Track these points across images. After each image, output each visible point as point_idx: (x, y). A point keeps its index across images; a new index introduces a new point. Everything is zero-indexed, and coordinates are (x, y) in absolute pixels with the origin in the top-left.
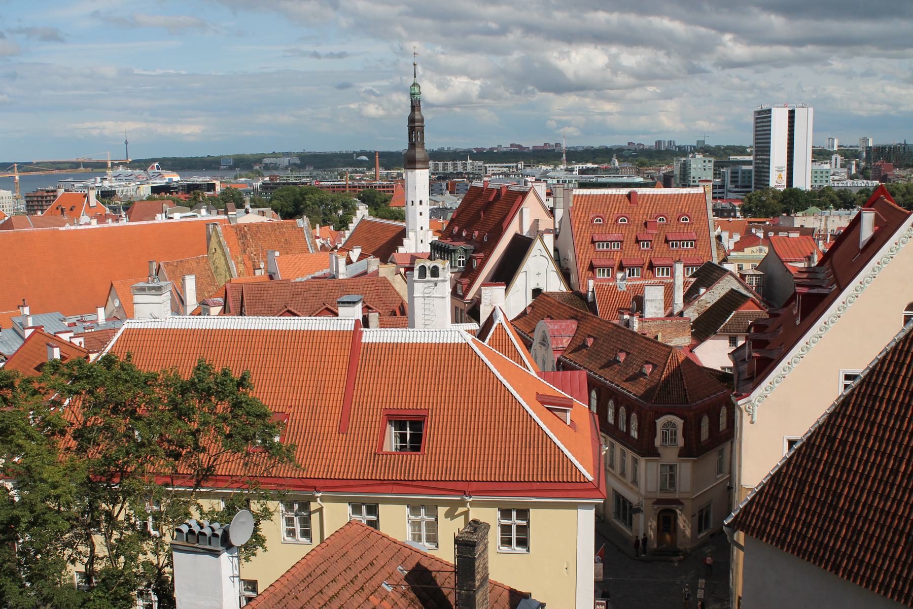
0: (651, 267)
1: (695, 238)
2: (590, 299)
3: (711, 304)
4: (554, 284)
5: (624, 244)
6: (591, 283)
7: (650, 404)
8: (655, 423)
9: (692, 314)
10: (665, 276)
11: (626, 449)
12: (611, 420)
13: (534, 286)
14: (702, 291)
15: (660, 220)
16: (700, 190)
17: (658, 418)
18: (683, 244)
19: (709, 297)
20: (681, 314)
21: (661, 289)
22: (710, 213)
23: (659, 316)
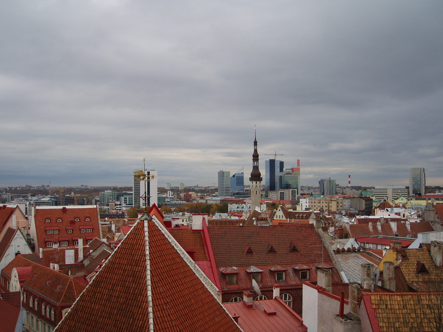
0: (73, 241)
1: (92, 228)
2: (41, 256)
3: (95, 257)
4: (26, 250)
5: (60, 231)
6: (41, 249)
7: (59, 304)
8: (62, 312)
9: (86, 263)
10: (77, 245)
11: (50, 325)
12: (43, 313)
13: (17, 252)
14: (91, 251)
15: (76, 220)
16: (95, 206)
17: (63, 309)
18: (87, 230)
19: (96, 254)
20: (82, 261)
21: (73, 251)
22: (99, 216)
23: (72, 263)
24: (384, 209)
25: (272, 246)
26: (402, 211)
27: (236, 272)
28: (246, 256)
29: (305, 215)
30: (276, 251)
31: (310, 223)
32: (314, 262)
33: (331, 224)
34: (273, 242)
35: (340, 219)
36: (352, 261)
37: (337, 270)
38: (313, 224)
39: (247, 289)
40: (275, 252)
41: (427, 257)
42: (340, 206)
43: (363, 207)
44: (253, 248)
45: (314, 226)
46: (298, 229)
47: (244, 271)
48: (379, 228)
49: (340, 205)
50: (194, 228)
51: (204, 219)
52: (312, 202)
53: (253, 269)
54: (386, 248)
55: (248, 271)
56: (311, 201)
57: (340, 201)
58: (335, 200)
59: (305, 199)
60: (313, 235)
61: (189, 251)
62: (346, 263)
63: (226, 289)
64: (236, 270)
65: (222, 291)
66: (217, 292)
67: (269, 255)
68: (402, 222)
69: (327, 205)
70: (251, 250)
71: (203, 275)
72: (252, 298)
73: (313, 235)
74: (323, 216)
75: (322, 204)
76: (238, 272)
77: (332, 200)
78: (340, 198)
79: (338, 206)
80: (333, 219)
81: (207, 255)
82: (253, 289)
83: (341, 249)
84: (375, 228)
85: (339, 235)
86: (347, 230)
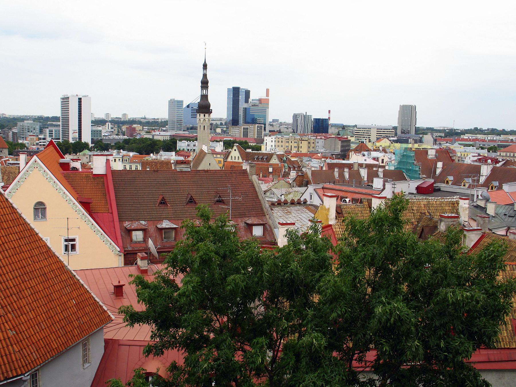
24: (360, 152)
25: (191, 196)
26: (379, 155)
27: (144, 227)
28: (158, 208)
29: (265, 157)
30: (197, 202)
31: (244, 168)
32: (243, 216)
33: (292, 169)
34: (194, 191)
35: (307, 163)
36: (294, 215)
37: (270, 227)
38: (246, 170)
39: (140, 251)
40: (195, 203)
41: (367, 215)
42: (311, 147)
43: (338, 150)
44: (168, 198)
45: (247, 172)
46: (227, 175)
47: (155, 226)
48: (347, 175)
49: (312, 145)
50: (95, 172)
51: (108, 161)
52: (279, 142)
53: (166, 224)
54: (346, 200)
55: (159, 226)
56: (277, 140)
57: (312, 141)
58: (306, 139)
59: (270, 138)
60: (246, 183)
61: (83, 201)
62: (287, 218)
63: (130, 249)
64: (145, 225)
65: (125, 251)
66: (117, 253)
67: (188, 206)
68: (374, 169)
69: (296, 145)
70: (165, 200)
71: (100, 232)
72: (146, 261)
73: (246, 183)
74: (287, 159)
75: (291, 144)
76: (146, 228)
77: (303, 139)
78: (312, 138)
79: (309, 147)
80: (299, 163)
81: (109, 206)
82: (150, 250)
83: (283, 200)
84: (341, 175)
85: (299, 183)
86: (308, 177)
